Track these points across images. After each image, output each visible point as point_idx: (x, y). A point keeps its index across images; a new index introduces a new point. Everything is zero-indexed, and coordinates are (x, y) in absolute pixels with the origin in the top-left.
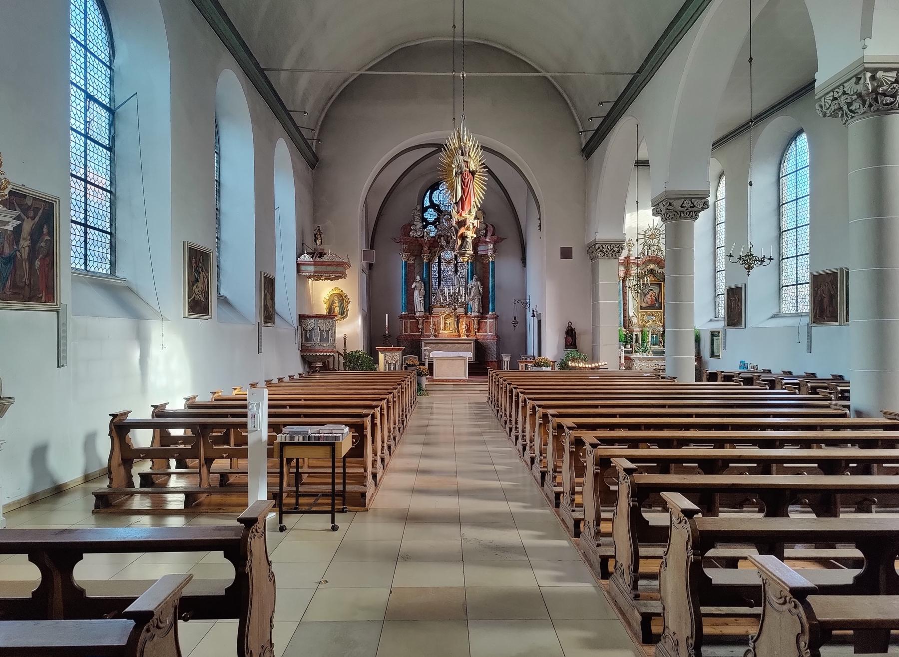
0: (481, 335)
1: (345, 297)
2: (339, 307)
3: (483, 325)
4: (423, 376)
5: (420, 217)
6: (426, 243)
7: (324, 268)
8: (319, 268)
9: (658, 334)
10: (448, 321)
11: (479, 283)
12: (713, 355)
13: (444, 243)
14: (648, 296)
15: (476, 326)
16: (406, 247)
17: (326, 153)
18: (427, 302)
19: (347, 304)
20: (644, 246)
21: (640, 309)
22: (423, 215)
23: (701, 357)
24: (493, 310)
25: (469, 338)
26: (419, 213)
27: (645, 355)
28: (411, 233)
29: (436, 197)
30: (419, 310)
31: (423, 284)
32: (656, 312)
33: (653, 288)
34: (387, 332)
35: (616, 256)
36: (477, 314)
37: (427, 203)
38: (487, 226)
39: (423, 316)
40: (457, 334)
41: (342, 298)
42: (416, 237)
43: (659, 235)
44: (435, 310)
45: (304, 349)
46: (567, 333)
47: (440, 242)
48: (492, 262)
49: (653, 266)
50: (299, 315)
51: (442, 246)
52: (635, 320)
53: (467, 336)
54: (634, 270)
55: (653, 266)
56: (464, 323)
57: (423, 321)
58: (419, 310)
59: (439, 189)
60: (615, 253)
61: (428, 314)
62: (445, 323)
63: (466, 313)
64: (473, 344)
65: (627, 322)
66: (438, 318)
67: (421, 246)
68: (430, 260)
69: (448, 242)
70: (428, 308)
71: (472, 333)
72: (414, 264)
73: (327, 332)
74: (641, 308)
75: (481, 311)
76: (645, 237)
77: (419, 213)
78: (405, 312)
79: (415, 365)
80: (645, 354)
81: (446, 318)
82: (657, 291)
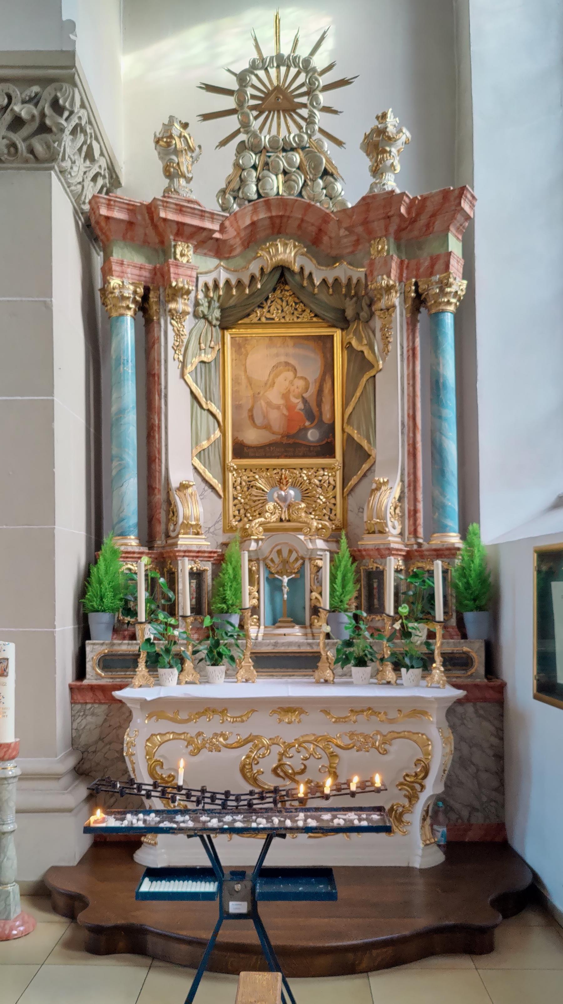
9: (301, 571)
35: (31, 151)
60: (26, 131)
76: (241, 103)
80: (218, 672)
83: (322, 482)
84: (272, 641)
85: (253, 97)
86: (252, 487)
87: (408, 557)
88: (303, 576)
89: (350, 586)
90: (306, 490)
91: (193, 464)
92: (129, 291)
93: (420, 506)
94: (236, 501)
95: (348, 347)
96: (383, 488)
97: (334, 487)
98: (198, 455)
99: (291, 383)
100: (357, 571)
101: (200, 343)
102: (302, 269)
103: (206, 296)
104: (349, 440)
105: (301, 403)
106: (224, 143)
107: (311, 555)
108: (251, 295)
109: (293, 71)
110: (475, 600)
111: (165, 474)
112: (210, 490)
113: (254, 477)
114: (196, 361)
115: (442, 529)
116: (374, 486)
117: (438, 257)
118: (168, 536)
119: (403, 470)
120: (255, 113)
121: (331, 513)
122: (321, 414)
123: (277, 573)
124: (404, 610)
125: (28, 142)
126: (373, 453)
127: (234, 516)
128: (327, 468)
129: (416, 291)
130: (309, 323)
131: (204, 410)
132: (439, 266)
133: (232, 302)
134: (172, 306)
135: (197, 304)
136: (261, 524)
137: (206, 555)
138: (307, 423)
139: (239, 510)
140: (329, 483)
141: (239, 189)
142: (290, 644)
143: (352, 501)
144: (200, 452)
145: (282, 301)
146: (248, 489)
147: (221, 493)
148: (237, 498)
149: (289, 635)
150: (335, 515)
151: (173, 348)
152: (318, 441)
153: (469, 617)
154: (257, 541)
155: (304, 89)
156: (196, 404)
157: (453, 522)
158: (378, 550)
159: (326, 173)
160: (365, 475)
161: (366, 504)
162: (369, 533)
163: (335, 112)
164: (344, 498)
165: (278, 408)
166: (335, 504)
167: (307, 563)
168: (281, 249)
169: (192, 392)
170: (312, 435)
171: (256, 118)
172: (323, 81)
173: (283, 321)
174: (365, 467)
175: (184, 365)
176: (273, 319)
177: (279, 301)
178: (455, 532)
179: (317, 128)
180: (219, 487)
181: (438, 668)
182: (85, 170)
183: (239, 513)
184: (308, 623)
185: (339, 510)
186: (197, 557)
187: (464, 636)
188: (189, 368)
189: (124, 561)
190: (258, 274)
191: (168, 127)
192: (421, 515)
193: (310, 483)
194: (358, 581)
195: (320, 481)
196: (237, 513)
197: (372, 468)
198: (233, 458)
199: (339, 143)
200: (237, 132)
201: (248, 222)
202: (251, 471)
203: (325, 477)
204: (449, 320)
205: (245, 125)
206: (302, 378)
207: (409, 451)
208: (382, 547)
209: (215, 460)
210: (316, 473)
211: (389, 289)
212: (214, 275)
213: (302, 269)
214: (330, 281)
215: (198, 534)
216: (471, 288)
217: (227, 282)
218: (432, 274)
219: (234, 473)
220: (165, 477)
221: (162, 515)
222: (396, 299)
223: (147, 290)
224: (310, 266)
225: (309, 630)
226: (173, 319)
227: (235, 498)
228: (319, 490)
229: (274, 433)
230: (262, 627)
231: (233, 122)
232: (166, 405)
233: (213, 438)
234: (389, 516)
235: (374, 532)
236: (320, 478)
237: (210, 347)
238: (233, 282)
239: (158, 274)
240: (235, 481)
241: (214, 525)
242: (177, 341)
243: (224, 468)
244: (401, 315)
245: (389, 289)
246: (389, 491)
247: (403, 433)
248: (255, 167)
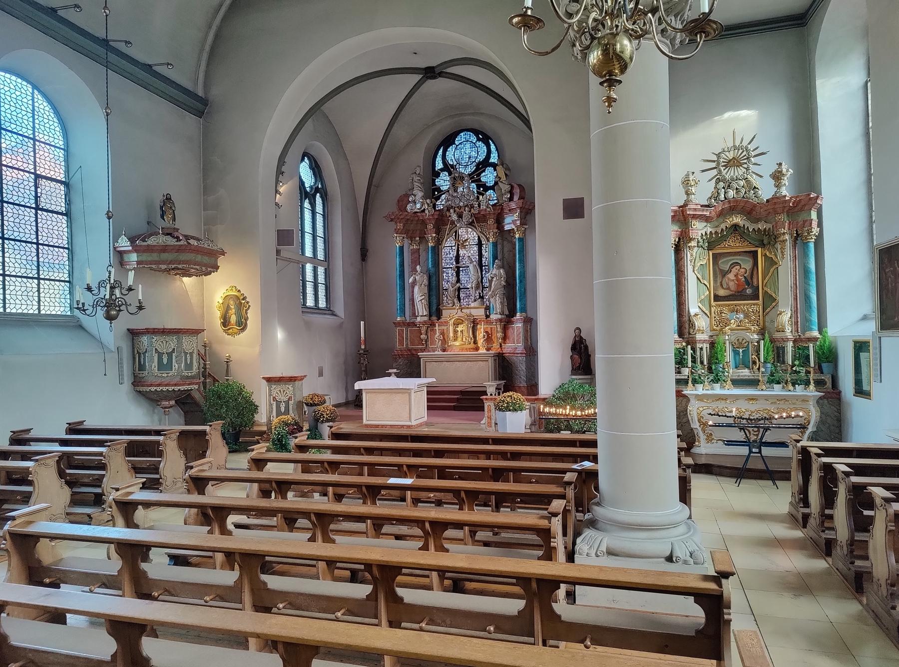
0: (508, 347)
1: (243, 299)
2: (235, 314)
3: (510, 332)
4: (322, 422)
5: (421, 184)
6: (429, 219)
7: (155, 256)
8: (145, 257)
9: (747, 347)
10: (459, 329)
11: (502, 271)
12: (860, 391)
13: (454, 217)
14: (731, 276)
15: (500, 335)
16: (400, 226)
17: (216, 92)
18: (434, 301)
19: (246, 310)
20: (717, 183)
22: (434, 181)
23: (840, 392)
24: (524, 310)
25: (490, 352)
26: (419, 178)
27: (717, 390)
28: (409, 207)
29: (452, 154)
30: (421, 314)
31: (425, 276)
33: (741, 260)
34: (363, 347)
36: (500, 316)
37: (439, 165)
38: (512, 187)
39: (425, 322)
40: (472, 346)
41: (240, 303)
42: (416, 212)
43: (748, 158)
44: (445, 313)
45: (137, 382)
46: (574, 348)
47: (450, 216)
48: (519, 238)
49: (737, 220)
50: (128, 330)
51: (453, 223)
52: (701, 323)
53: (488, 349)
54: (699, 229)
55: (737, 220)
56: (482, 330)
57: (428, 328)
58: (421, 314)
59: (455, 144)
61: (434, 318)
62: (455, 332)
63: (487, 316)
64: (491, 362)
65: (684, 327)
66: (447, 323)
67: (424, 223)
68: (439, 242)
69: (460, 216)
70: (435, 311)
71: (496, 346)
72: (419, 249)
73: (170, 355)
74: (717, 298)
75: (507, 312)
77: (419, 178)
78: (400, 316)
79: (316, 405)
80: (717, 386)
81: (456, 324)
82: (747, 265)
85: (723, 162)
87: (795, 341)
88: (748, 349)
89: (770, 353)
93: (799, 320)
94: (715, 319)
96: (783, 314)
99: (739, 270)
100: (773, 347)
102: (744, 225)
103: (702, 238)
106: (710, 180)
108: (721, 237)
109: (741, 151)
110: (826, 358)
114: (699, 264)
115: (811, 330)
116: (779, 312)
117: (806, 221)
118: (689, 334)
119: (791, 305)
120: (724, 168)
123: (737, 348)
124: (797, 363)
127: (715, 325)
129: (797, 233)
132: (807, 224)
134: (690, 245)
135: (698, 242)
141: (717, 197)
142: (745, 376)
143: (767, 318)
147: (709, 316)
149: (744, 372)
152: (752, 293)
153: (824, 365)
154: (728, 335)
155: (746, 157)
156: (699, 282)
157: (815, 327)
159: (755, 188)
163: (759, 165)
165: (733, 280)
167: (750, 343)
168: (735, 218)
170: (749, 291)
171: (724, 170)
172: (753, 154)
173: (735, 246)
175: (694, 267)
177: (734, 238)
179: (751, 171)
180: (709, 314)
181: (812, 387)
184: (751, 368)
185: (761, 322)
187: (822, 373)
188: (696, 268)
190: (724, 229)
191: (687, 175)
192: (799, 323)
194: (773, 351)
200: (717, 175)
201: (720, 209)
204: (812, 246)
205: (720, 172)
207: (794, 298)
208: (784, 337)
211: (784, 233)
212: (705, 230)
213: (744, 225)
214: (756, 229)
215: (703, 333)
216: (821, 232)
221: (687, 326)
222: (787, 237)
224: (747, 224)
225: (752, 370)
228: (752, 314)
231: (715, 172)
232: (687, 283)
233: (706, 294)
234: (786, 325)
235: (779, 331)
238: (713, 232)
239: (684, 233)
244: (790, 243)
245: (784, 233)
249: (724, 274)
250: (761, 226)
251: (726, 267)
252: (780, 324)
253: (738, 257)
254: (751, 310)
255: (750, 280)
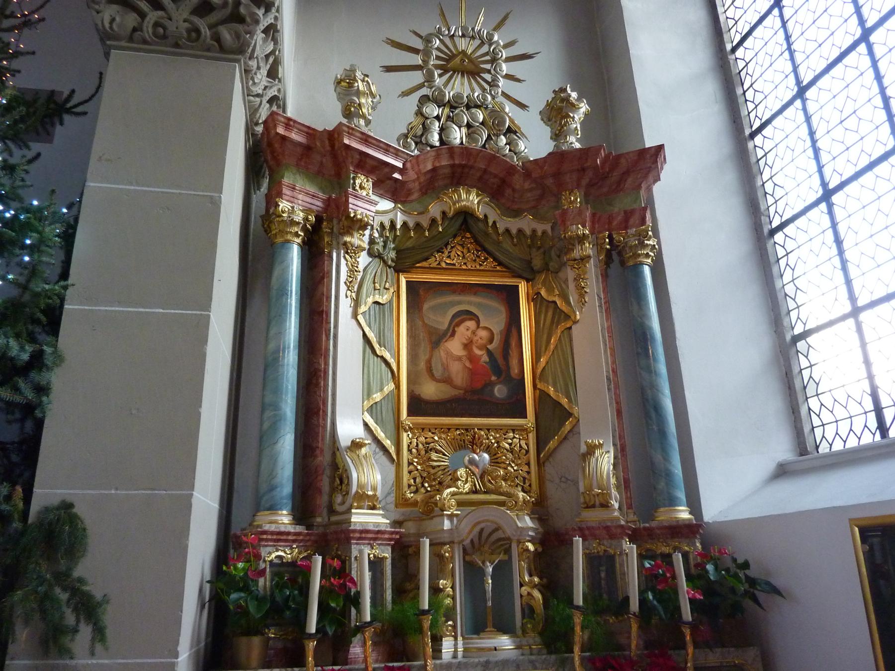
14: (455, 346)
21: (410, 413)
32: (497, 429)
33: (479, 305)
35: (217, 38)
49: (471, 199)
55: (471, 199)
60: (213, 18)
82: (496, 322)
83: (513, 445)
84: (482, 660)
85: (438, 58)
86: (431, 450)
90: (496, 455)
91: (363, 420)
92: (299, 217)
94: (411, 467)
95: (535, 299)
96: (597, 452)
97: (527, 452)
98: (370, 409)
99: (474, 333)
101: (374, 283)
102: (486, 216)
103: (381, 235)
104: (542, 398)
105: (485, 355)
106: (406, 94)
107: (520, 536)
108: (429, 239)
111: (331, 429)
112: (381, 453)
113: (433, 438)
114: (370, 300)
115: (672, 502)
117: (632, 212)
118: (332, 511)
120: (440, 72)
121: (524, 483)
122: (508, 368)
125: (214, 30)
126: (575, 410)
127: (409, 486)
128: (518, 430)
129: (610, 243)
130: (493, 271)
131: (378, 356)
133: (409, 244)
134: (348, 239)
135: (372, 242)
136: (453, 494)
137: (387, 536)
138: (493, 378)
139: (415, 479)
140: (520, 446)
141: (422, 135)
143: (549, 469)
144: (372, 405)
145: (463, 247)
146: (426, 452)
147: (395, 457)
148: (412, 464)
150: (530, 485)
151: (345, 283)
154: (451, 517)
155: (488, 58)
156: (368, 350)
158: (607, 528)
160: (565, 438)
161: (580, 472)
162: (587, 507)
163: (518, 80)
164: (540, 464)
165: (459, 359)
166: (528, 473)
168: (464, 196)
169: (364, 335)
170: (500, 391)
171: (440, 76)
173: (464, 267)
174: (568, 425)
175: (357, 303)
176: (454, 265)
177: (459, 248)
178: (684, 506)
179: (500, 91)
180: (392, 450)
182: (266, 84)
183: (415, 482)
186: (375, 539)
188: (363, 309)
189: (275, 546)
190: (439, 218)
193: (499, 447)
195: (510, 444)
196: (412, 481)
197: (576, 429)
198: (409, 415)
199: (522, 106)
200: (421, 86)
202: (430, 431)
203: (515, 439)
205: (429, 79)
206: (486, 328)
209: (389, 417)
210: (505, 435)
211: (582, 239)
212: (391, 216)
213: (486, 216)
214: (514, 231)
217: (405, 224)
218: (626, 228)
219: (409, 433)
220: (330, 433)
221: (325, 483)
222: (588, 249)
223: (319, 219)
226: (347, 253)
227: (410, 463)
228: (510, 456)
229: (455, 387)
230: (460, 638)
231: (417, 77)
235: (593, 506)
236: (510, 441)
237: (385, 288)
238: (411, 224)
239: (333, 205)
240: (411, 443)
241: (386, 497)
242: (350, 277)
243: (399, 427)
245: (582, 239)
246: (606, 456)
247: (609, 389)
248: (438, 118)
249: (438, 338)
250: (526, 223)
251: (443, 322)
252: (595, 484)
253: (473, 299)
254: (507, 446)
255: (501, 361)
